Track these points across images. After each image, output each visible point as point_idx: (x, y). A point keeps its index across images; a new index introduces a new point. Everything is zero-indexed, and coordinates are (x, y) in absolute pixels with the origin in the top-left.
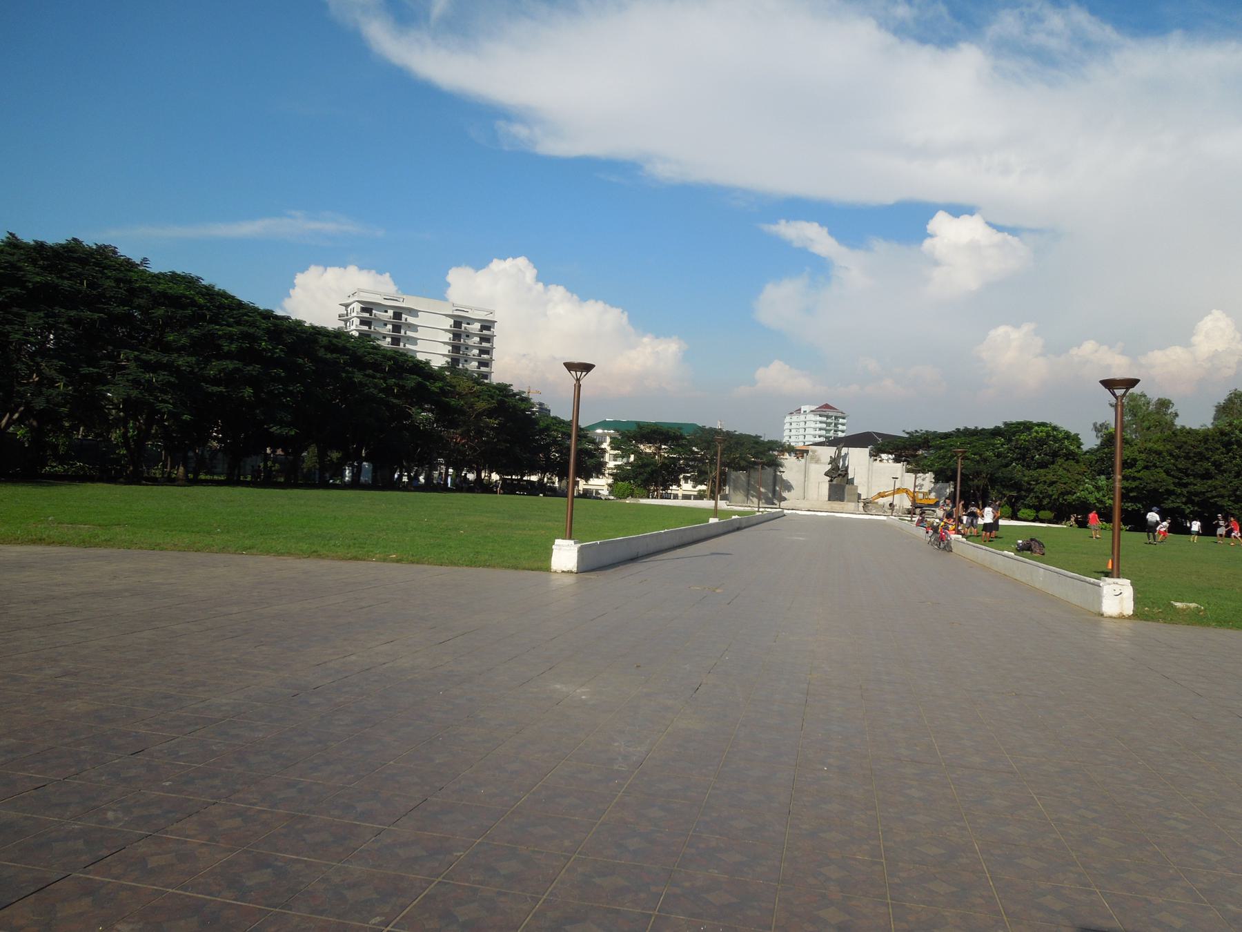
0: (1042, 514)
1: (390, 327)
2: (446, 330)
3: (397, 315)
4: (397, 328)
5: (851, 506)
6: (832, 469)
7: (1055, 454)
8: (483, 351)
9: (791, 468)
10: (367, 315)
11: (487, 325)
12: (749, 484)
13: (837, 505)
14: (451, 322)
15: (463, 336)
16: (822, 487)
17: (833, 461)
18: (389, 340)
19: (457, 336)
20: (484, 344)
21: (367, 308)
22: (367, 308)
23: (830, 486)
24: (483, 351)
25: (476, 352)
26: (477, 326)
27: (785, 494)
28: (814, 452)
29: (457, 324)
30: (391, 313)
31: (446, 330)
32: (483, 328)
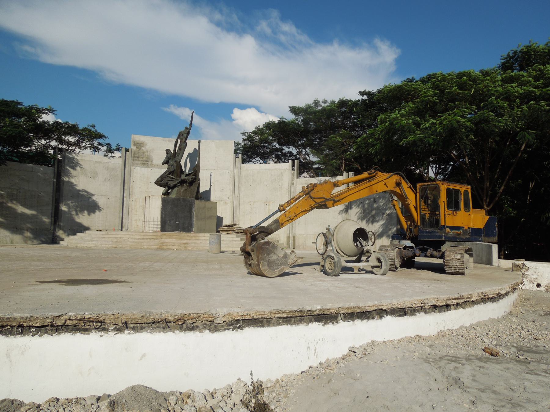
5: (200, 241)
6: (170, 173)
9: (91, 171)
13: (174, 240)
16: (148, 202)
17: (172, 158)
23: (164, 201)
27: (83, 219)
28: (139, 145)
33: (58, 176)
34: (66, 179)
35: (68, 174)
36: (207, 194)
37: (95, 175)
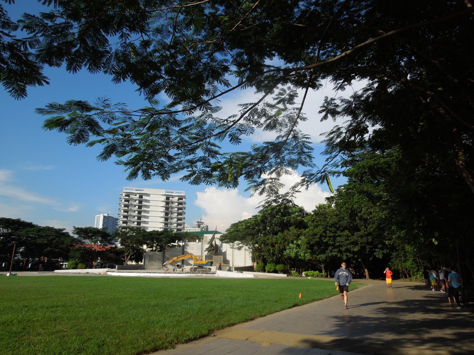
0: (279, 267)
1: (137, 202)
2: (162, 201)
3: (141, 197)
4: (140, 202)
7: (285, 226)
8: (179, 209)
10: (127, 197)
11: (180, 198)
12: (164, 256)
14: (165, 197)
15: (170, 203)
18: (137, 207)
19: (167, 203)
20: (180, 206)
21: (128, 195)
22: (128, 195)
24: (179, 209)
25: (176, 209)
26: (177, 198)
28: (206, 237)
29: (168, 198)
30: (138, 196)
31: (162, 201)
32: (179, 199)
33: (183, 250)
34: (185, 250)
35: (186, 249)
36: (226, 252)
37: (193, 249)
